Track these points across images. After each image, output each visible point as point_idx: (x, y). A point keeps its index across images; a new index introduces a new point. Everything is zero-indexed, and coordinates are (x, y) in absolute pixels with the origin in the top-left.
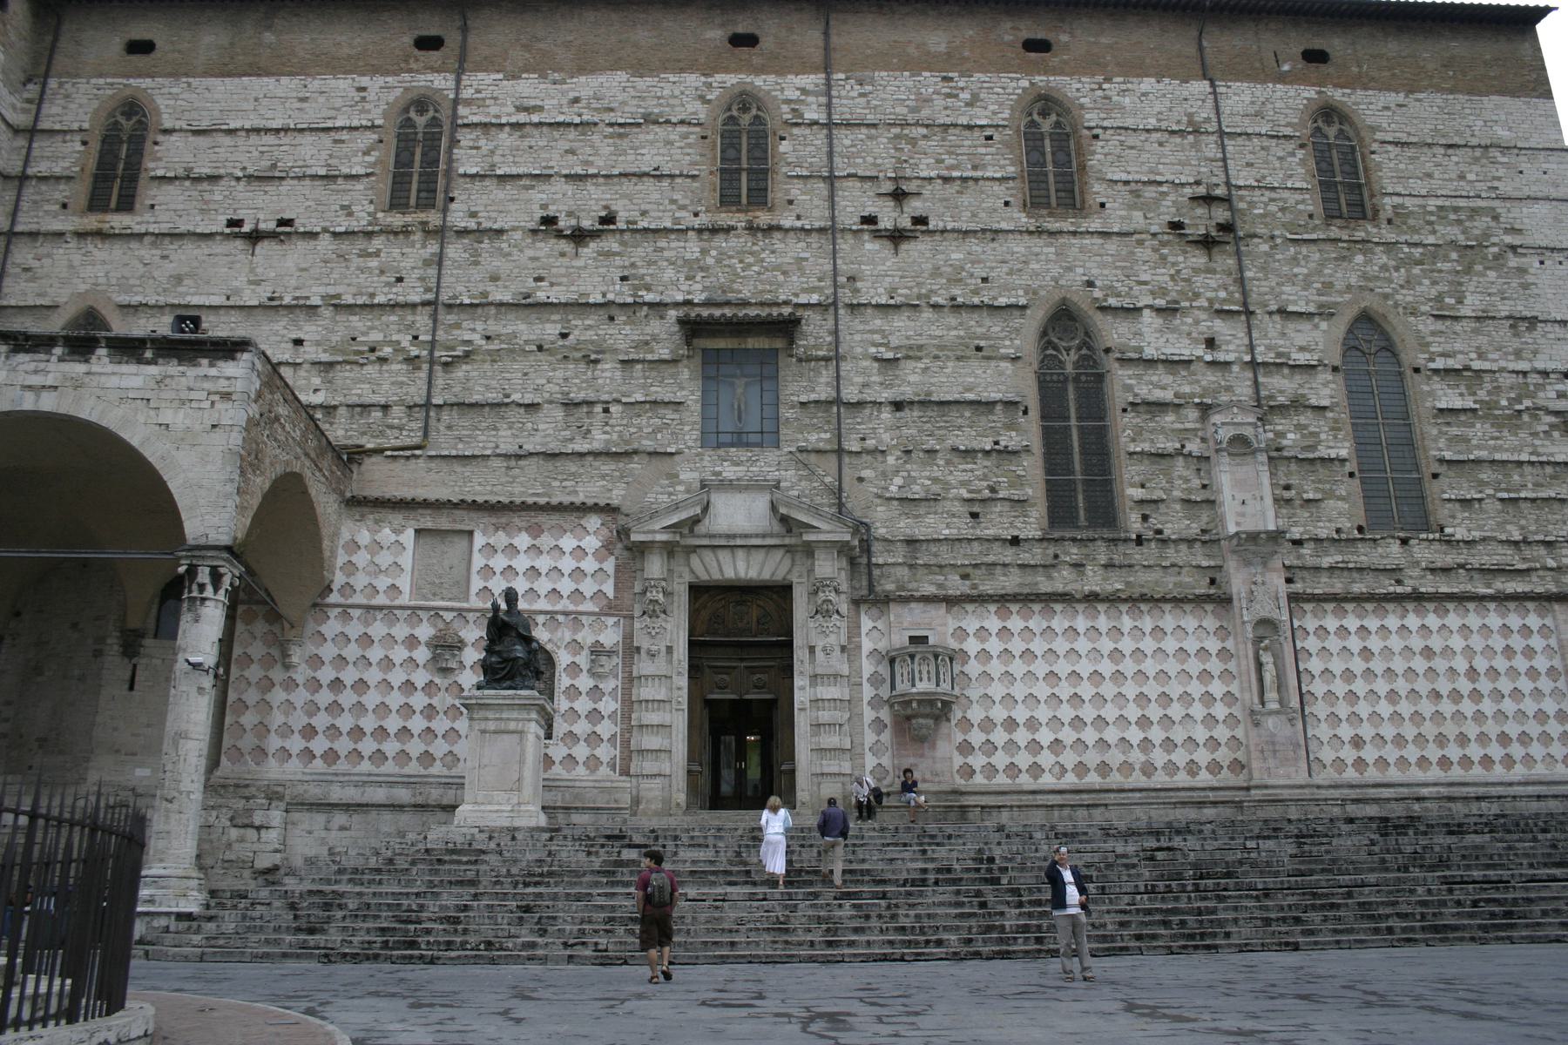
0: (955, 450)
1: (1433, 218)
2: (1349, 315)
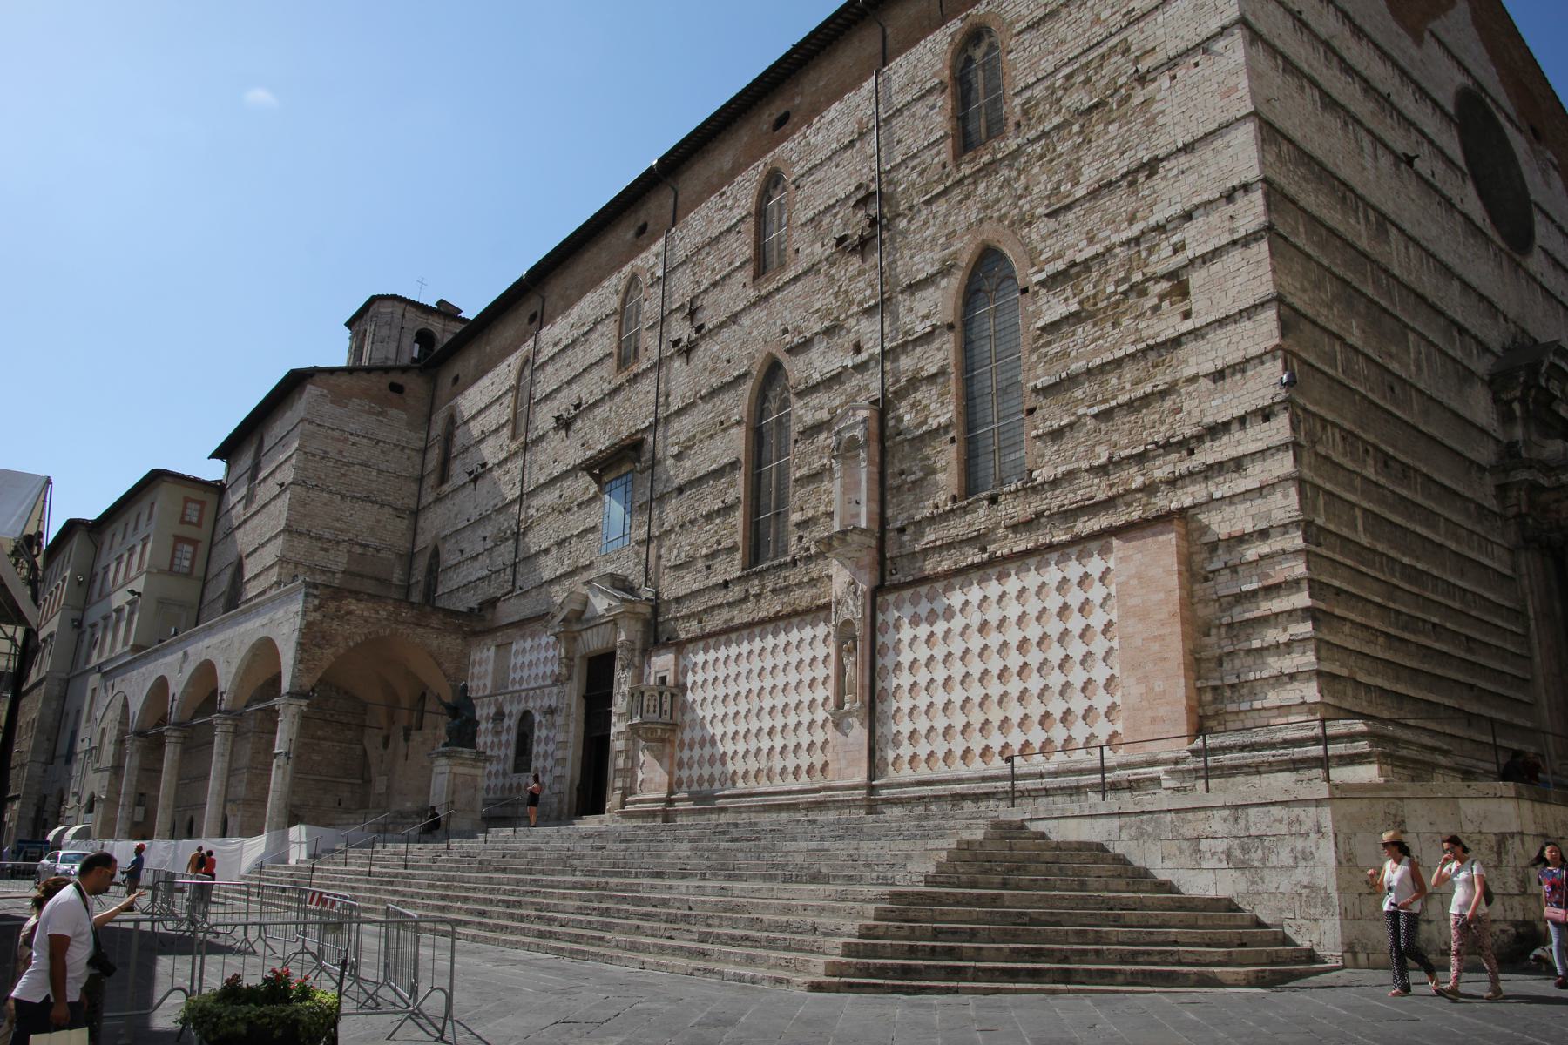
1: (1059, 94)
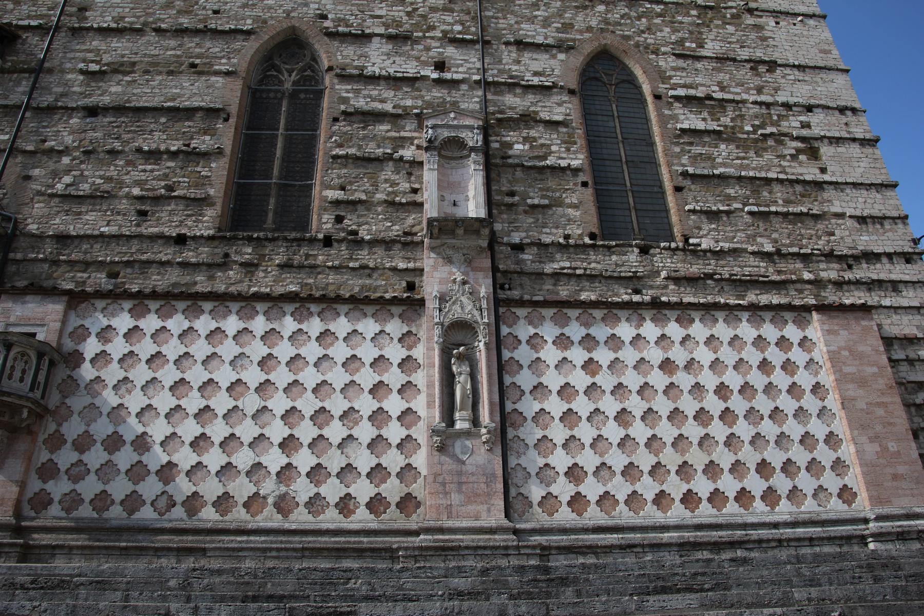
0: (139, 150)
2: (588, 49)
